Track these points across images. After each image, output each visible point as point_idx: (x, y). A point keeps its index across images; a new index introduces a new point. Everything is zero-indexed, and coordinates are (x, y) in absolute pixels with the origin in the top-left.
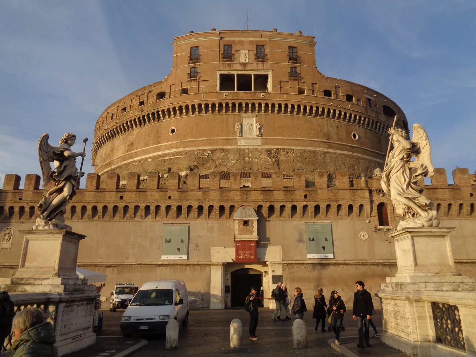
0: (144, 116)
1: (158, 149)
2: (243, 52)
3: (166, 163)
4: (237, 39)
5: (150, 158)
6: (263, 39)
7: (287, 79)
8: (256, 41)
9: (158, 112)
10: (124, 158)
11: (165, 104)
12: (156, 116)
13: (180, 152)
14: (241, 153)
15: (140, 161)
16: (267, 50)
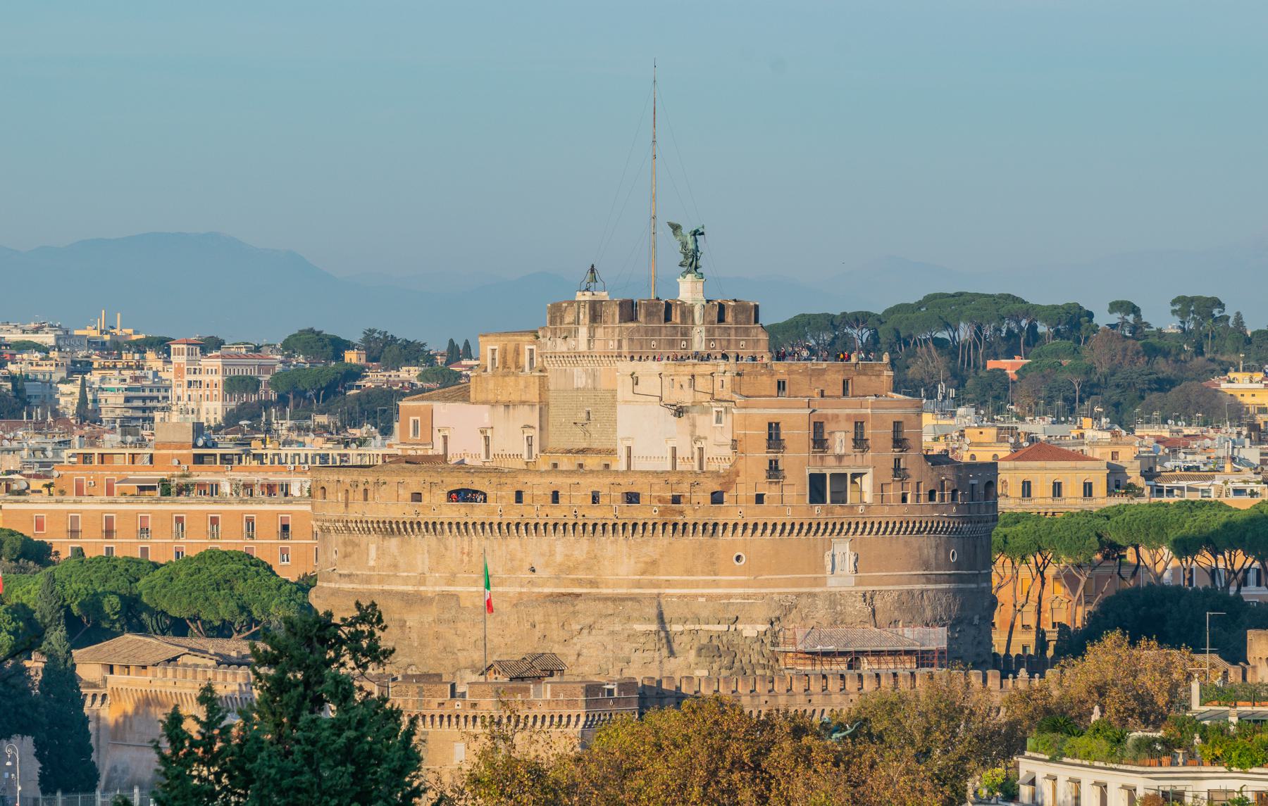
0: (685, 524)
1: (716, 584)
2: (838, 435)
3: (731, 608)
4: (830, 412)
5: (702, 596)
6: (863, 411)
7: (890, 480)
8: (856, 416)
9: (715, 525)
10: (638, 584)
11: (729, 513)
12: (713, 529)
13: (755, 595)
14: (833, 600)
15: (680, 597)
16: (868, 432)
